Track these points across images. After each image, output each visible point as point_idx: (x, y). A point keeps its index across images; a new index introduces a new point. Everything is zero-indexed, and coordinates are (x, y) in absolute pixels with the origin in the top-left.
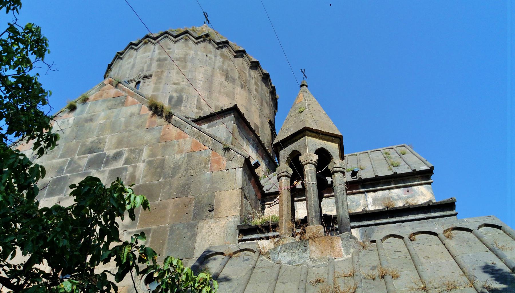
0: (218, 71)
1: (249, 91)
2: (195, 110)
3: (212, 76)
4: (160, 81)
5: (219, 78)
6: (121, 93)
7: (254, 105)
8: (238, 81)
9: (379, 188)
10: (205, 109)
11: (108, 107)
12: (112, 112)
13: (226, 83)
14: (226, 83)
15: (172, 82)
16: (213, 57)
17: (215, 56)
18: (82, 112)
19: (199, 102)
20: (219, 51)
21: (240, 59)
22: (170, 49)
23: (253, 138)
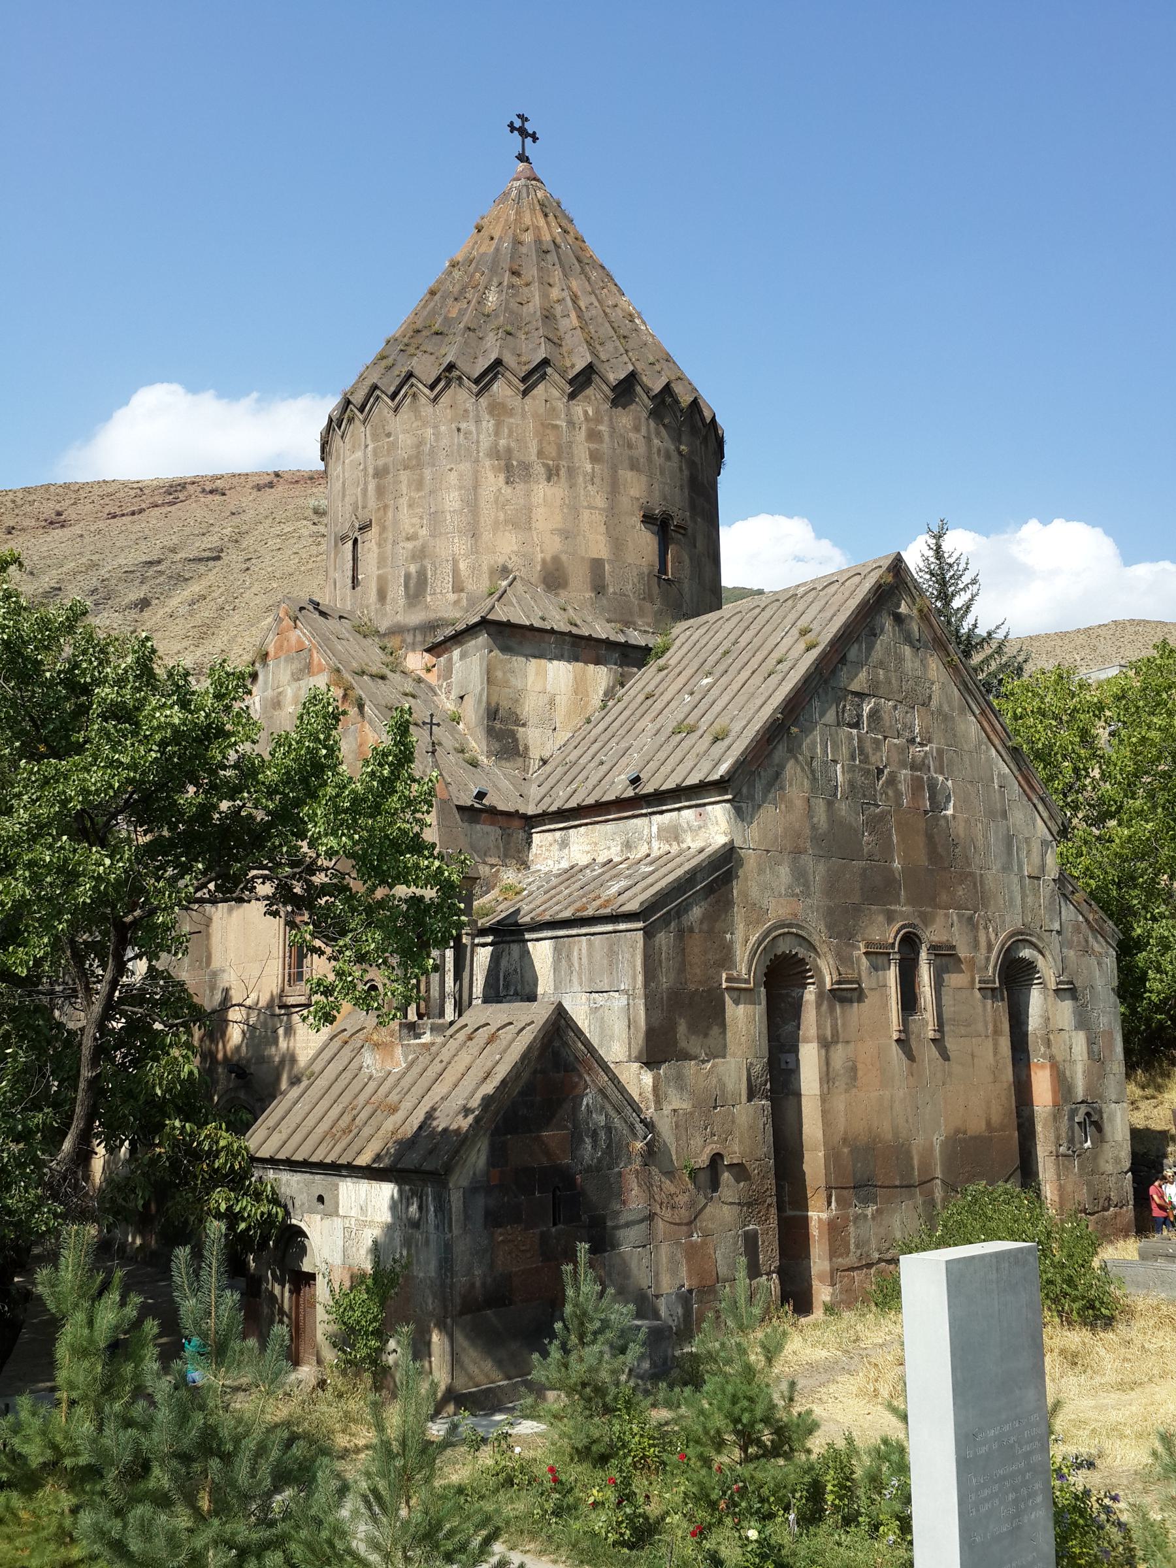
0: (488, 463)
1: (571, 472)
2: (452, 597)
3: (476, 487)
4: (384, 536)
5: (493, 482)
6: (303, 643)
7: (590, 507)
8: (539, 469)
9: (664, 808)
10: (470, 587)
11: (293, 674)
12: (300, 688)
13: (509, 490)
14: (507, 491)
15: (404, 534)
16: (473, 429)
17: (478, 421)
18: (266, 683)
19: (456, 571)
20: (483, 401)
21: (541, 387)
22: (389, 435)
23: (555, 642)
